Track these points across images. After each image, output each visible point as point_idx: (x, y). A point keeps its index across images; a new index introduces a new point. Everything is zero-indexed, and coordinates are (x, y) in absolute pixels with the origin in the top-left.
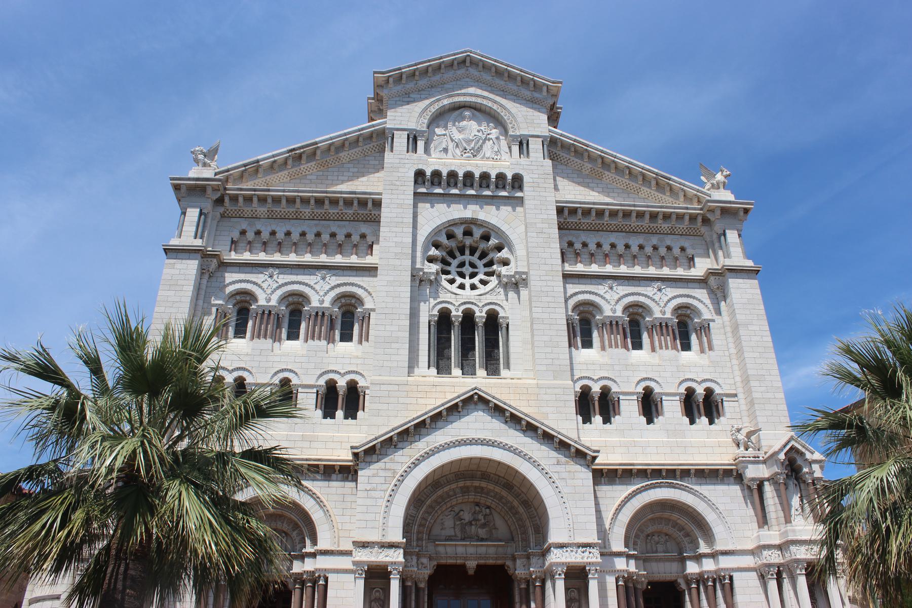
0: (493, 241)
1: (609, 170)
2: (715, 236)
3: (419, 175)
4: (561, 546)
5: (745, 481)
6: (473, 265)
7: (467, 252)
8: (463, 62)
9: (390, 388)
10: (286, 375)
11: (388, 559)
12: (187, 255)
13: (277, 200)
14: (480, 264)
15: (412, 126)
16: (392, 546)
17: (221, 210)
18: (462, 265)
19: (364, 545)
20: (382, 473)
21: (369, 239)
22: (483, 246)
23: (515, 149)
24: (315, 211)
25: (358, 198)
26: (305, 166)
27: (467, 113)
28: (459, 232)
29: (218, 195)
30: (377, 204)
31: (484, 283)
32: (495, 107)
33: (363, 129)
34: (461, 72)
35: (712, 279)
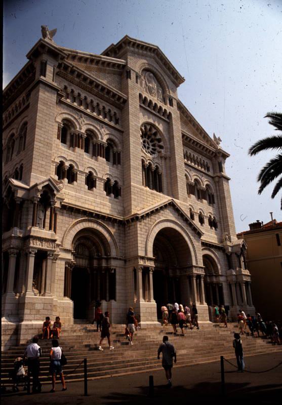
0: (158, 137)
1: (191, 123)
2: (217, 162)
3: (140, 95)
4: (195, 267)
5: (226, 252)
6: (148, 144)
7: (147, 137)
8: (155, 50)
9: (138, 190)
10: (91, 170)
11: (149, 265)
12: (50, 90)
13: (85, 79)
14: (151, 144)
15: (136, 70)
16: (149, 259)
17: (58, 70)
18: (144, 142)
19: (142, 258)
20: (145, 227)
21: (118, 116)
22: (153, 137)
23: (168, 102)
24: (100, 92)
25: (119, 96)
26: (94, 66)
27: (152, 75)
28: (148, 127)
29: (60, 62)
30: (125, 102)
31: (154, 153)
32: (162, 78)
33: (118, 61)
34: (153, 55)
35: (217, 178)
